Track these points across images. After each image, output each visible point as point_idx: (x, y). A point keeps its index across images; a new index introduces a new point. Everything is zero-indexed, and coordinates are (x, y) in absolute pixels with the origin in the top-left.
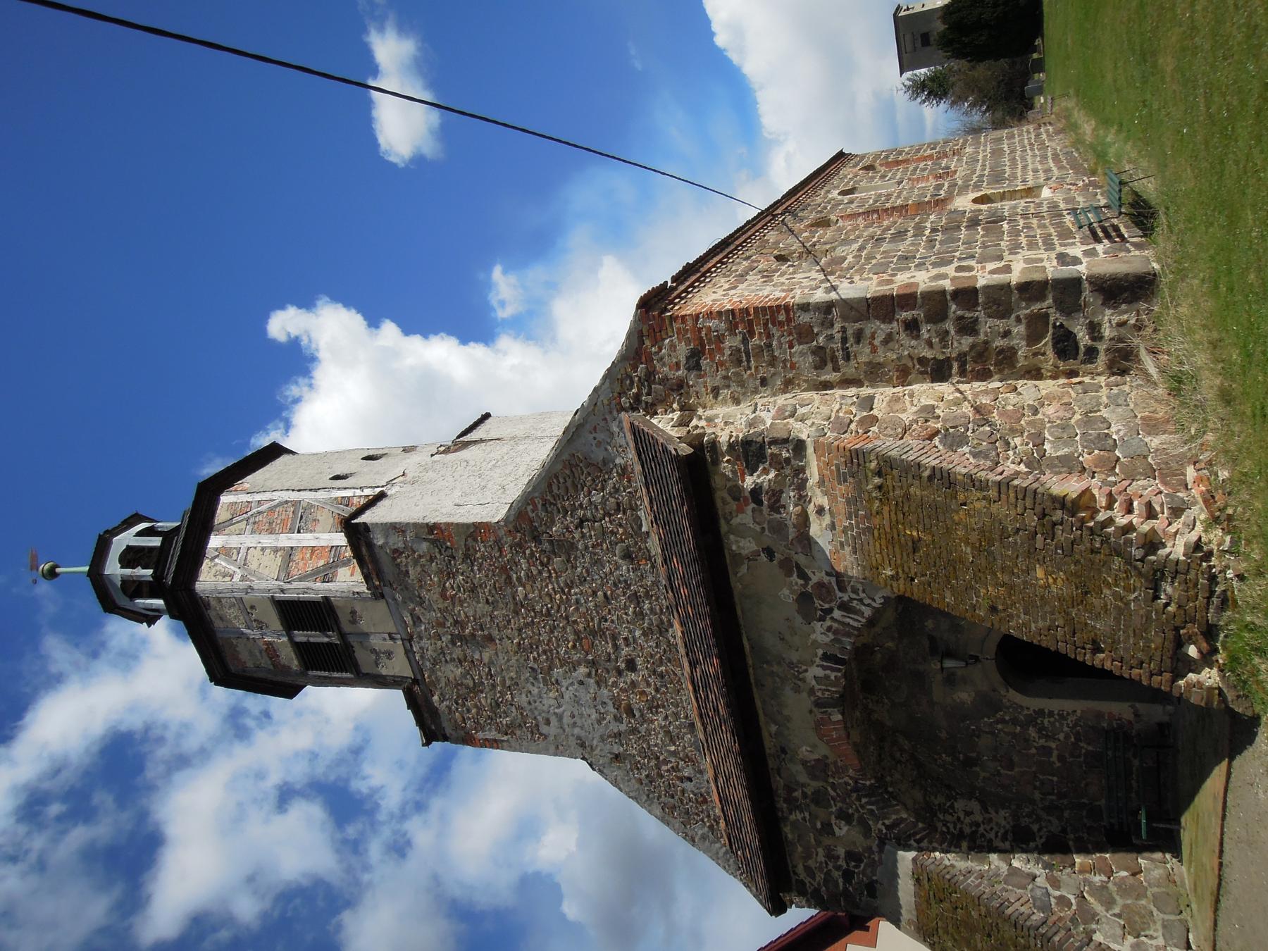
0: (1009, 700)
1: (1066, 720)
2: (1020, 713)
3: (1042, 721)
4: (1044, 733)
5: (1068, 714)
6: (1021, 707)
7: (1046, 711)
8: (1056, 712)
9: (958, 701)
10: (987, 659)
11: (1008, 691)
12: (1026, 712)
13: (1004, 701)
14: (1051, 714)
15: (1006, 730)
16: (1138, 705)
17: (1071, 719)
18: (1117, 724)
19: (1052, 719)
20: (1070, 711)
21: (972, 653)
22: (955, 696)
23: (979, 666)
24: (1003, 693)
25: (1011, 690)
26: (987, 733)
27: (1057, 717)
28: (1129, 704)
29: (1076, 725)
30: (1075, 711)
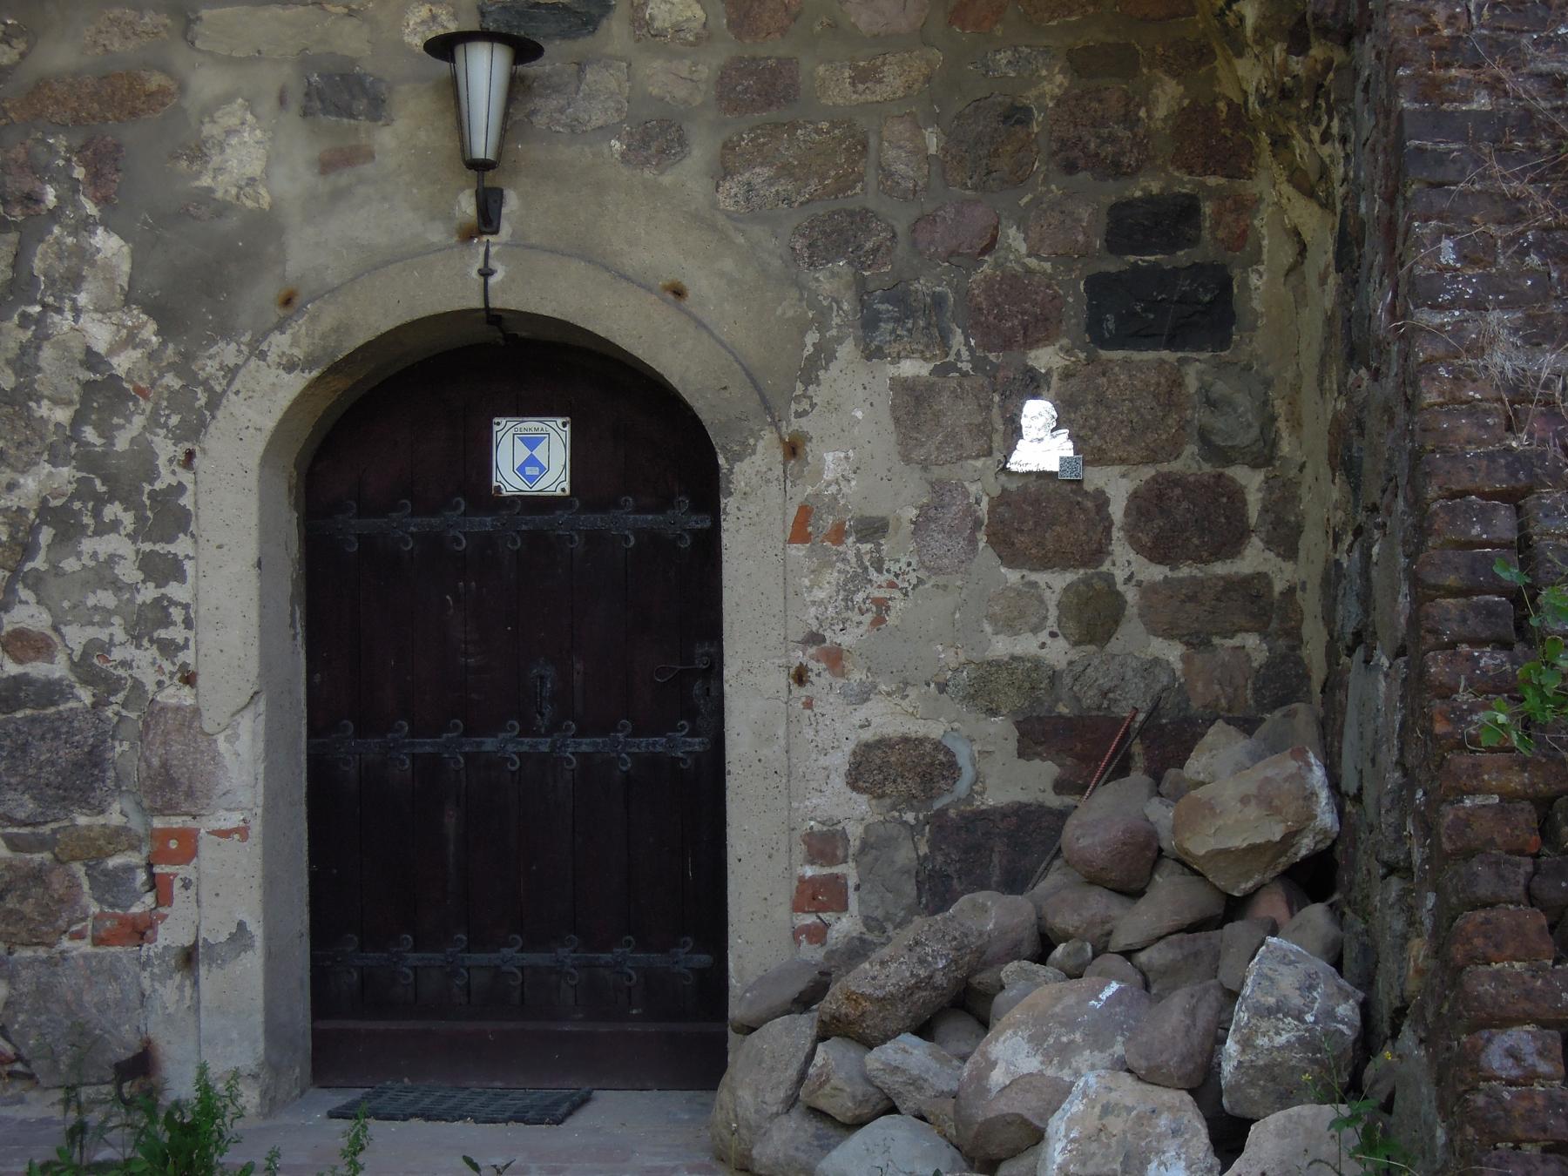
0: (232, 372)
1: (136, 640)
2: (154, 421)
3: (115, 526)
4: (46, 535)
5: (168, 648)
6: (193, 430)
7: (181, 546)
8: (174, 590)
9: (208, 129)
10: (486, 273)
11: (290, 367)
12: (165, 449)
13: (228, 352)
14: (164, 570)
15: (47, 354)
16: (252, 963)
17: (144, 663)
18: (129, 869)
19: (128, 572)
20: (187, 657)
21: (512, 203)
22: (231, 115)
23: (437, 234)
24: (279, 343)
25: (297, 382)
26: (20, 259)
27: (149, 593)
28: (256, 929)
29: (105, 684)
30: (189, 679)
